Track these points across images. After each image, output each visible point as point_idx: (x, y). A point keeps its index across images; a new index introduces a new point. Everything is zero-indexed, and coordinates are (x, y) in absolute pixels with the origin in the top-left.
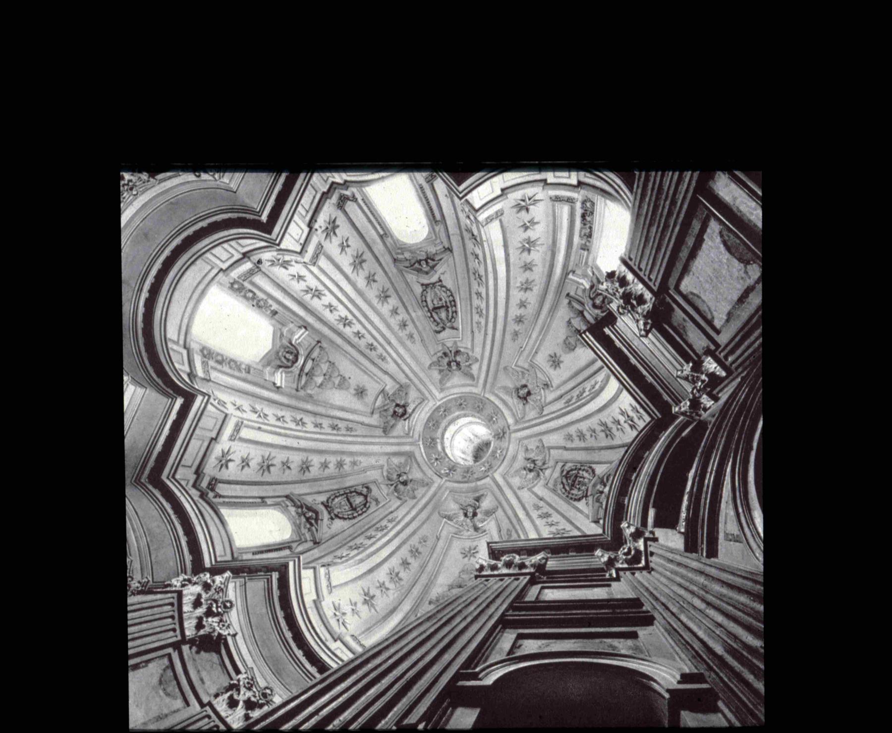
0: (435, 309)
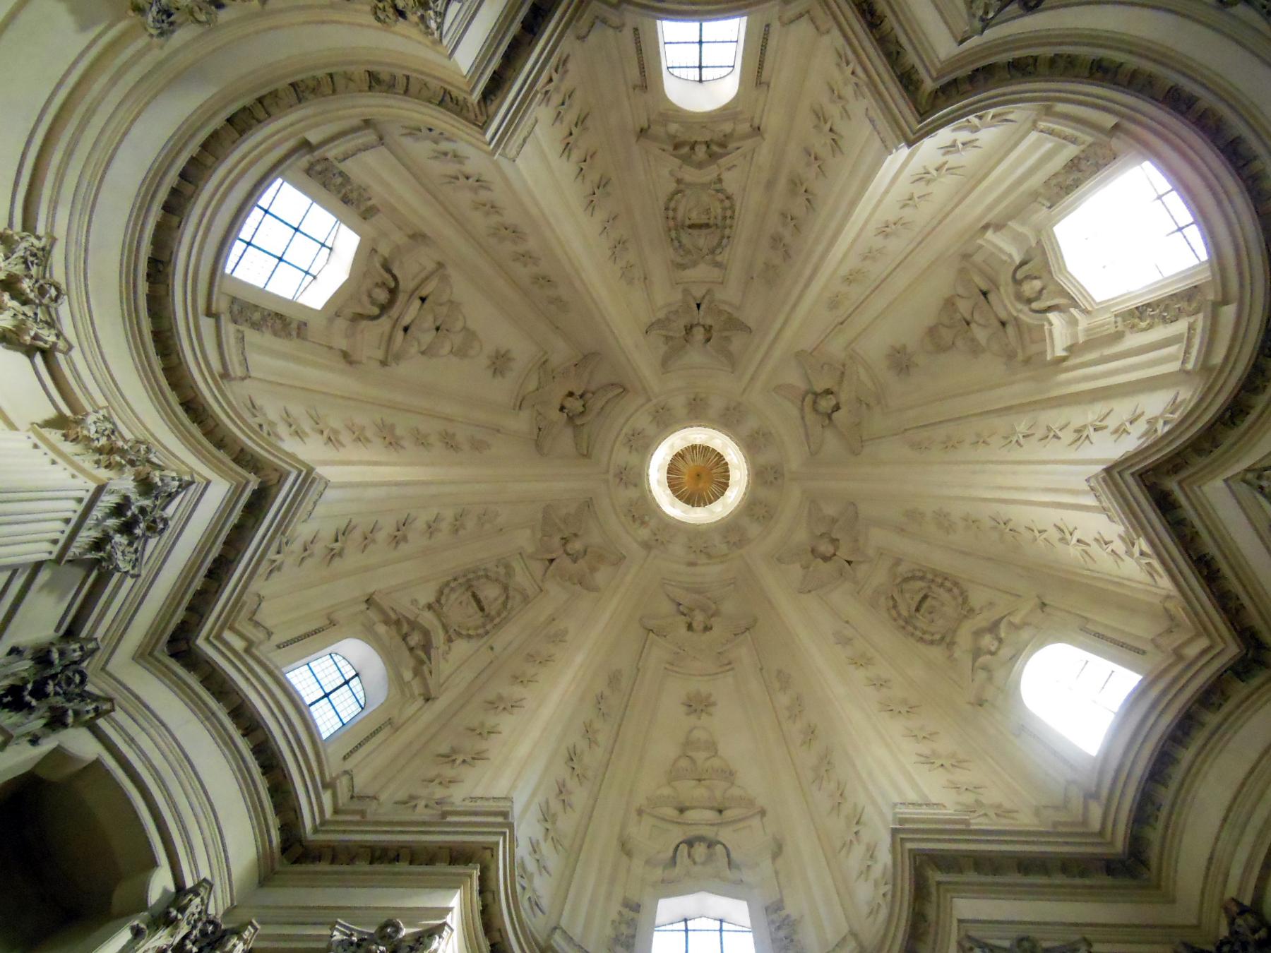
0: (690, 227)
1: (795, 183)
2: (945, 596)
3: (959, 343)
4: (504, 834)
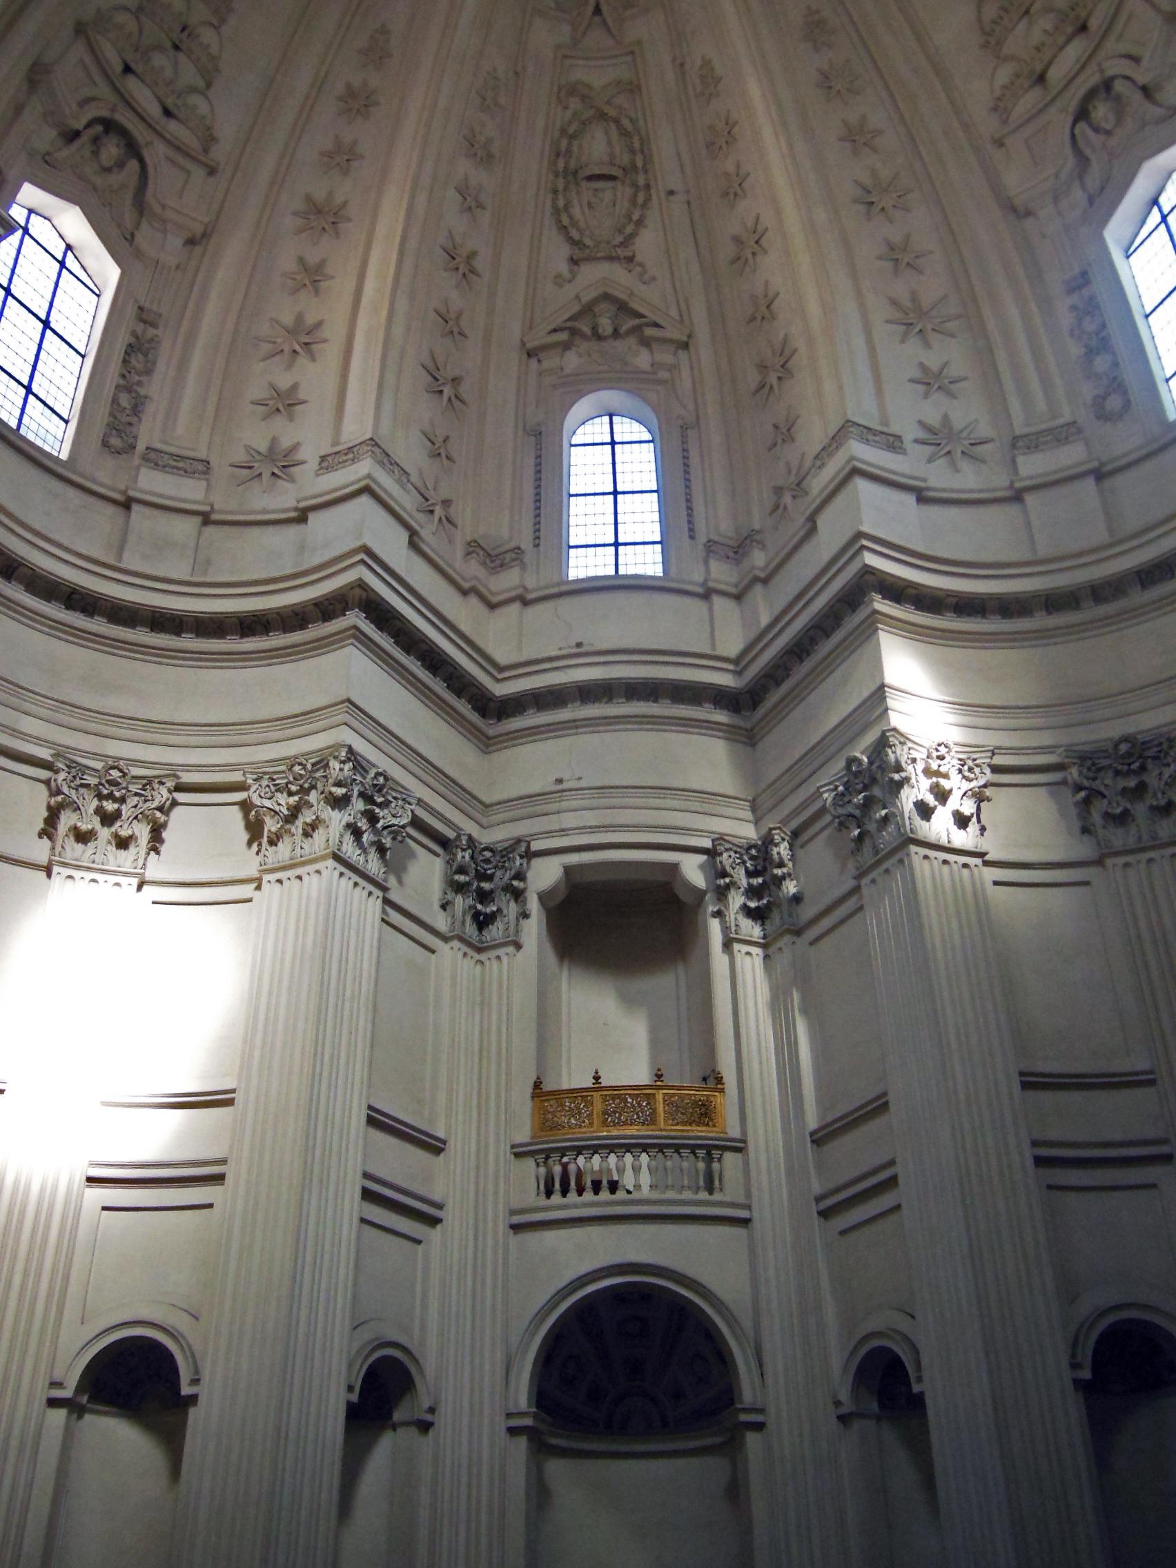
4: (863, 547)
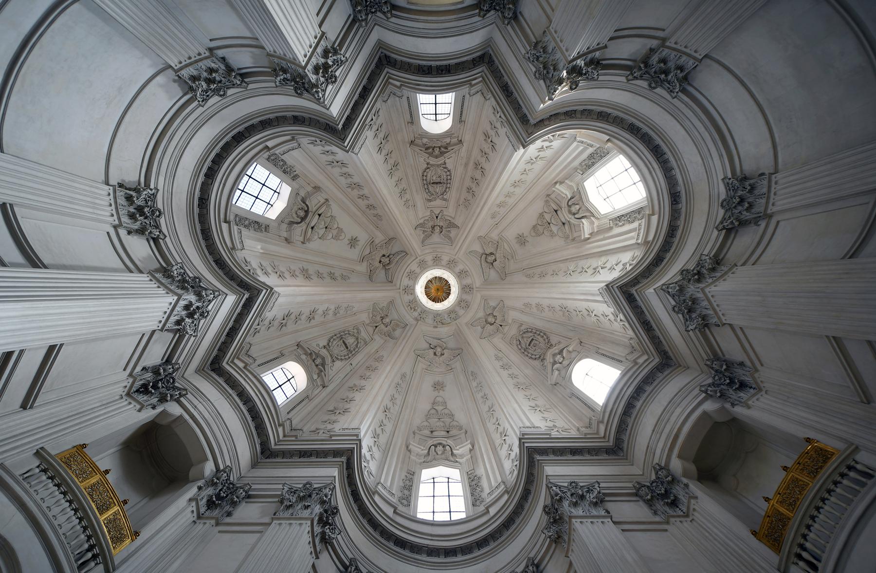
1: (477, 165)
2: (541, 339)
3: (545, 232)
